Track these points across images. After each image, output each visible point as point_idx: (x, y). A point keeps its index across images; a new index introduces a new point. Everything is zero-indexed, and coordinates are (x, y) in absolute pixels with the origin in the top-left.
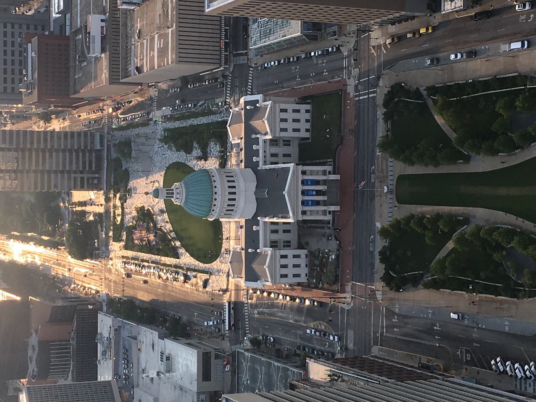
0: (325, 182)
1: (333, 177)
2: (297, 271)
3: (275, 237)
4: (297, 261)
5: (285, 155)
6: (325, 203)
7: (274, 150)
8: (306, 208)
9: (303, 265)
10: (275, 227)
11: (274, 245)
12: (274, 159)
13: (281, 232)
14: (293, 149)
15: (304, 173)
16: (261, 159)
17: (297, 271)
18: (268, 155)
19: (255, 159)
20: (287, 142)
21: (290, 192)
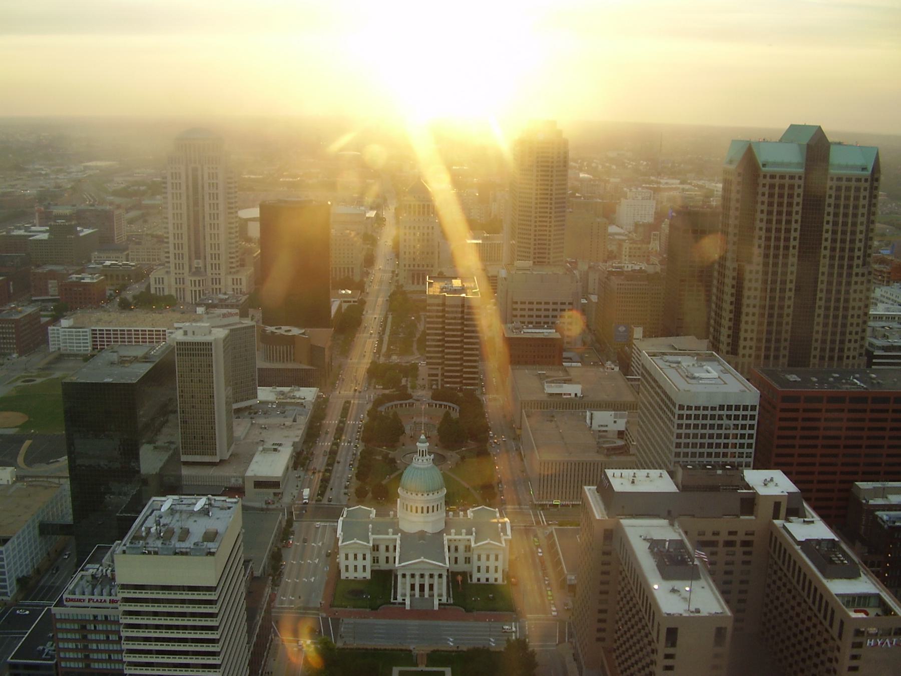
0: (432, 596)
1: (436, 602)
2: (351, 568)
3: (382, 548)
4: (360, 568)
5: (456, 558)
6: (412, 596)
9: (356, 575)
10: (391, 548)
11: (376, 548)
12: (453, 549)
13: (387, 554)
14: (461, 567)
15: (440, 576)
16: (453, 537)
17: (351, 568)
18: (456, 544)
20: (468, 560)
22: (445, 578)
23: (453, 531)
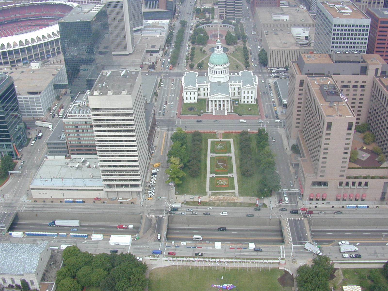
0: (224, 109)
1: (226, 112)
5: (234, 93)
6: (216, 109)
7: (236, 89)
8: (214, 102)
12: (233, 89)
14: (236, 96)
15: (228, 101)
16: (233, 84)
19: (233, 81)
20: (239, 94)
21: (220, 96)
22: (229, 101)
23: (233, 81)
